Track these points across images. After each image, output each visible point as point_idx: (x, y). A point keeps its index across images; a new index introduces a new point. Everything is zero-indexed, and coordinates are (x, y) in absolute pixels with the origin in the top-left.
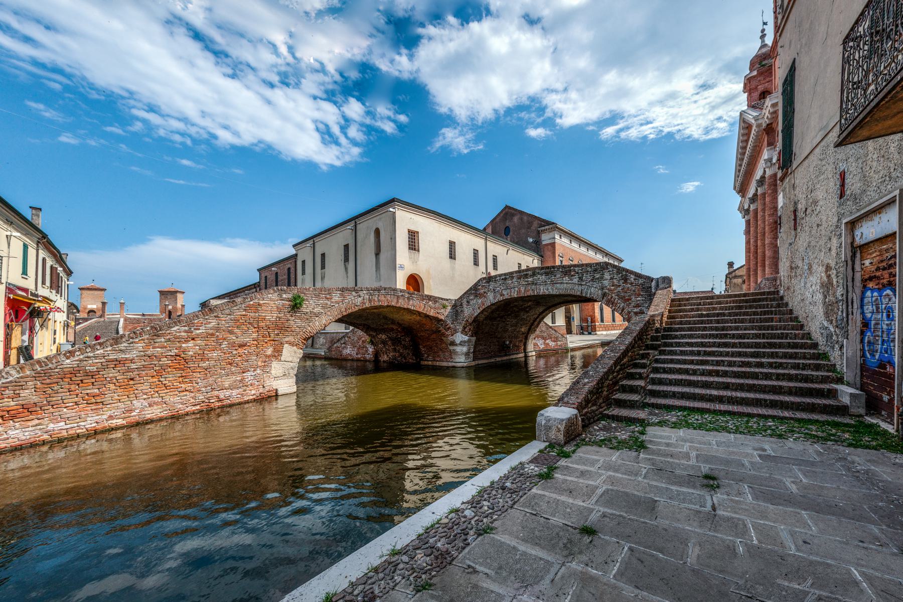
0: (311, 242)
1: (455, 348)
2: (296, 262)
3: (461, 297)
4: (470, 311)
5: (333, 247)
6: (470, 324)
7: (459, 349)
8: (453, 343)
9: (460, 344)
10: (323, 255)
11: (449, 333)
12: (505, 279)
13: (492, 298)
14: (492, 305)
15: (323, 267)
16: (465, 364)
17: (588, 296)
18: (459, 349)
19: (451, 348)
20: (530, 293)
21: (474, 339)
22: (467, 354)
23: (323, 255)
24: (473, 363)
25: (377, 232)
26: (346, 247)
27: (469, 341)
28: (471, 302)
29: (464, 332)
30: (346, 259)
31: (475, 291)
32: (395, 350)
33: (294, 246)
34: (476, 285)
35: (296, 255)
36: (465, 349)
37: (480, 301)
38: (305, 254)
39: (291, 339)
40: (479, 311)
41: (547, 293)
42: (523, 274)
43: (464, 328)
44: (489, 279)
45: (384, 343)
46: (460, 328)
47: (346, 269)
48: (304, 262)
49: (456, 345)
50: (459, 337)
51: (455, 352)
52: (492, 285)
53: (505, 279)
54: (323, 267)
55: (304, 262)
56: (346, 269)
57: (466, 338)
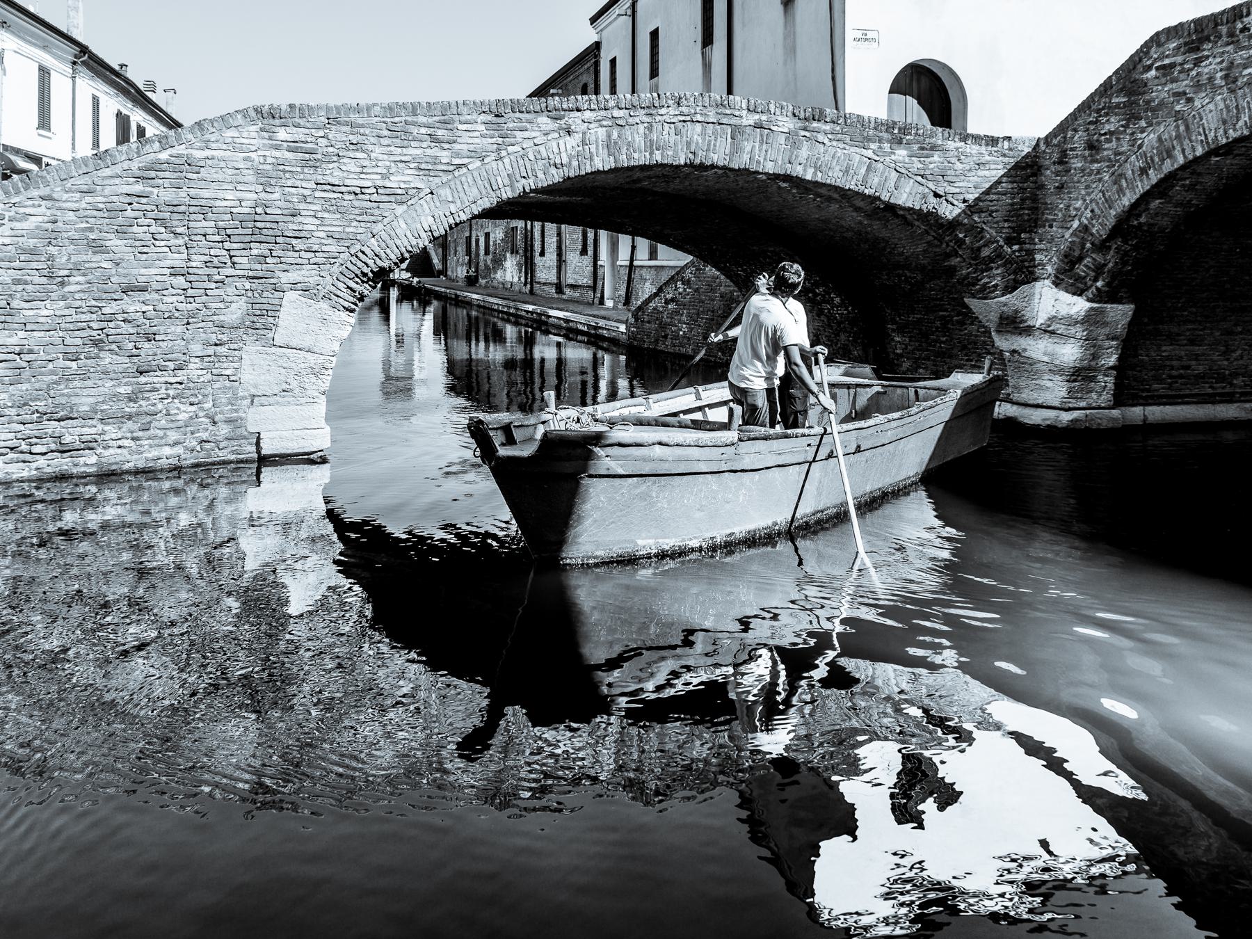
1: (1021, 343)
2: (597, 64)
6: (1102, 246)
9: (1048, 331)
10: (655, 35)
14: (1216, 151)
15: (654, 73)
18: (1037, 348)
19: (1003, 343)
23: (655, 35)
28: (1108, 149)
29: (1068, 279)
35: (597, 45)
40: (1142, 187)
46: (1048, 261)
47: (707, 66)
48: (613, 62)
50: (1049, 301)
54: (654, 73)
55: (613, 62)
56: (707, 66)
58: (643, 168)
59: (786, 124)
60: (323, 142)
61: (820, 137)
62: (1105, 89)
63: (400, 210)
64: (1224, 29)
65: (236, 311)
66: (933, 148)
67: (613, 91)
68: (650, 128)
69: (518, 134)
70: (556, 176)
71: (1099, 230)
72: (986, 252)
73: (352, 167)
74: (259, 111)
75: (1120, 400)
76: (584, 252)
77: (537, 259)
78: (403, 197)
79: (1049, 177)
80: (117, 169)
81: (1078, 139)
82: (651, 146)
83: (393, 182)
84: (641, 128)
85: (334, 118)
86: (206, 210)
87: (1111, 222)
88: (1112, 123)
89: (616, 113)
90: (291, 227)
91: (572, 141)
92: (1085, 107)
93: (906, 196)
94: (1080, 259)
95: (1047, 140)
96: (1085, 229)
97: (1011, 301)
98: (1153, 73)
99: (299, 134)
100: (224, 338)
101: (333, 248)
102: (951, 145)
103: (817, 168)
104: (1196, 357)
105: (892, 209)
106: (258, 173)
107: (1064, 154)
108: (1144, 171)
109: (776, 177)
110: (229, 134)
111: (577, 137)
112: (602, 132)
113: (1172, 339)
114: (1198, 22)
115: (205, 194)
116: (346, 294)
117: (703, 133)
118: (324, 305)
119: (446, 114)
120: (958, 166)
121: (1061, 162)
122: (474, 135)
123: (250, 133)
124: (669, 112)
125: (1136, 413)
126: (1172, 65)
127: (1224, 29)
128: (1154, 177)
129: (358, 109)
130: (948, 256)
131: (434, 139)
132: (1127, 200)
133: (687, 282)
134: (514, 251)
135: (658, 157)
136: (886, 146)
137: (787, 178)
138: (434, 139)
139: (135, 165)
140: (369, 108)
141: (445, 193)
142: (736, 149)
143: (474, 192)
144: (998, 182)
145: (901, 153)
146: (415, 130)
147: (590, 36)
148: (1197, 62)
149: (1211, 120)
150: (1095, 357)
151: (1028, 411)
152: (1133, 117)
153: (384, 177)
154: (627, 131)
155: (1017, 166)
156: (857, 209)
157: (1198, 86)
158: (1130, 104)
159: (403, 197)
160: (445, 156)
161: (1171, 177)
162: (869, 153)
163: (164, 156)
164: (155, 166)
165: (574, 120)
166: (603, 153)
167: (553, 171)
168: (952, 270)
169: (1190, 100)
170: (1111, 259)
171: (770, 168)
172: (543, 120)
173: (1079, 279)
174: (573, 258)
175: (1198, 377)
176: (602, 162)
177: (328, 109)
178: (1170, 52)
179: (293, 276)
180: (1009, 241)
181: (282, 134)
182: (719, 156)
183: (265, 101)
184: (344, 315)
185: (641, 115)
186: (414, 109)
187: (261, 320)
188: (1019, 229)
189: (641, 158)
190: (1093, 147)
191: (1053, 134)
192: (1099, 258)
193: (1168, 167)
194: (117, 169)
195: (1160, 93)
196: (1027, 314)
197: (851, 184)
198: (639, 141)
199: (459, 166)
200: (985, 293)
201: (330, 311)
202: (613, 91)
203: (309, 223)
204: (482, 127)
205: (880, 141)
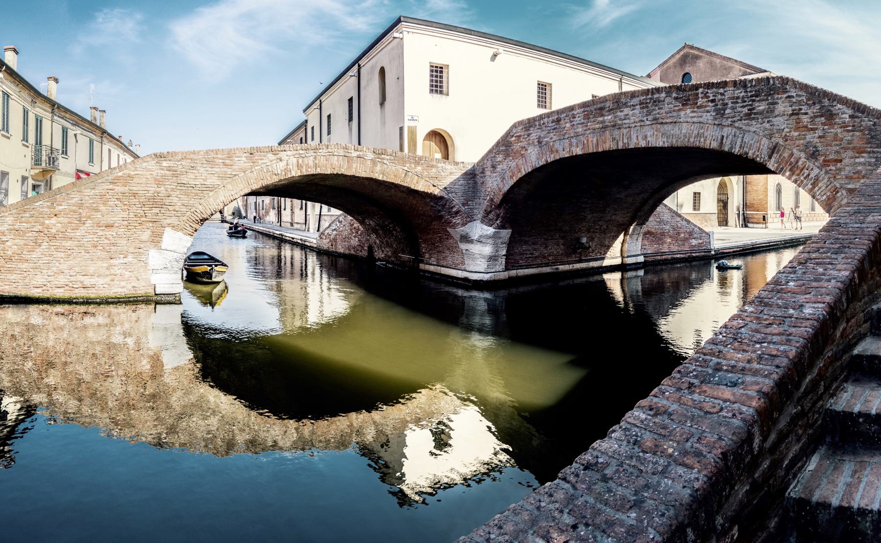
0: (318, 102)
3: (483, 159)
4: (496, 184)
5: (336, 104)
6: (499, 207)
7: (475, 248)
8: (466, 239)
10: (329, 116)
11: (457, 220)
12: (558, 121)
13: (534, 158)
14: (536, 171)
15: (329, 133)
16: (486, 277)
17: (726, 149)
20: (608, 145)
21: (506, 233)
22: (492, 258)
23: (329, 116)
24: (504, 275)
25: (382, 71)
26: (351, 100)
27: (495, 236)
28: (499, 168)
29: (487, 219)
30: (351, 119)
31: (505, 146)
32: (388, 245)
33: (305, 111)
34: (508, 134)
35: (306, 121)
36: (488, 250)
37: (513, 164)
38: (313, 122)
39: (174, 221)
41: (643, 144)
42: (596, 107)
43: (487, 213)
44: (529, 124)
45: (375, 231)
47: (350, 130)
48: (313, 128)
49: (471, 242)
50: (480, 229)
51: (472, 256)
52: (534, 136)
53: (558, 121)
54: (329, 133)
55: (313, 128)
56: (350, 130)
57: (490, 230)
58: (313, 175)
59: (370, 156)
60: (180, 167)
61: (385, 161)
62: (498, 144)
63: (211, 194)
64: (537, 123)
65: (146, 235)
66: (432, 166)
67: (313, 139)
68: (315, 158)
69: (260, 162)
70: (275, 180)
71: (497, 200)
72: (454, 210)
73: (192, 176)
74: (155, 155)
75: (507, 269)
76: (302, 208)
77: (283, 212)
78: (211, 188)
79: (479, 180)
80: (103, 180)
81: (489, 164)
82: (316, 166)
83: (208, 182)
84: (312, 158)
85: (185, 156)
86: (135, 195)
87: (500, 197)
88: (500, 158)
89: (301, 152)
90: (167, 201)
91: (282, 165)
92: (490, 151)
93: (421, 187)
94: (491, 212)
95: (478, 164)
96: (492, 200)
97: (466, 229)
98: (514, 138)
99: (171, 164)
100: (142, 246)
101: (184, 209)
102: (440, 165)
103: (383, 174)
104: (535, 250)
105: (416, 192)
106: (156, 180)
107: (484, 169)
108: (511, 177)
109: (367, 179)
110: (145, 164)
111: (284, 163)
112: (295, 160)
113: (526, 243)
114: (529, 119)
115: (135, 188)
116: (189, 229)
117: (338, 160)
118: (180, 234)
119: (230, 154)
120: (443, 174)
121: (483, 173)
122: (242, 161)
123: (152, 164)
124: (323, 151)
125: (513, 273)
126: (520, 136)
127: (537, 123)
128: (515, 179)
129: (194, 153)
130: (440, 211)
131: (225, 164)
132: (506, 188)
133: (340, 222)
134: (274, 208)
135: (319, 171)
136: (413, 166)
137: (371, 179)
138: (225, 164)
139: (110, 178)
140: (199, 152)
141: (229, 187)
142: (349, 167)
143: (241, 186)
144: (458, 180)
145: (419, 168)
146: (217, 161)
147: (303, 117)
148: (529, 135)
149: (533, 158)
150: (497, 251)
151: (473, 274)
152: (507, 155)
153: (204, 180)
154: (306, 160)
155: (466, 174)
156: (403, 192)
157: (529, 144)
158: (507, 150)
159: (211, 188)
160: (229, 171)
161: (521, 179)
162: (406, 168)
163: (120, 174)
164: (118, 178)
165: (283, 155)
166: (295, 168)
167: (274, 176)
168: (442, 217)
169: (526, 150)
170: (502, 212)
171: (363, 174)
172: (270, 155)
173: (490, 220)
174: (297, 210)
175: (536, 257)
176: (294, 174)
177: (182, 153)
178: (519, 131)
179: (168, 221)
180: (464, 205)
181: (165, 164)
182: (343, 171)
183: (158, 151)
184: (188, 237)
185: (311, 153)
186: (217, 152)
187: (156, 239)
188: (467, 200)
189: (312, 171)
190: (494, 167)
191: (480, 162)
192: (498, 211)
193: (520, 176)
194: (103, 180)
195: (516, 147)
196: (471, 234)
197: (398, 181)
198: (311, 163)
199: (235, 175)
200: (454, 226)
201: (183, 236)
202: (313, 139)
203: (175, 200)
204: (244, 159)
205: (410, 163)
